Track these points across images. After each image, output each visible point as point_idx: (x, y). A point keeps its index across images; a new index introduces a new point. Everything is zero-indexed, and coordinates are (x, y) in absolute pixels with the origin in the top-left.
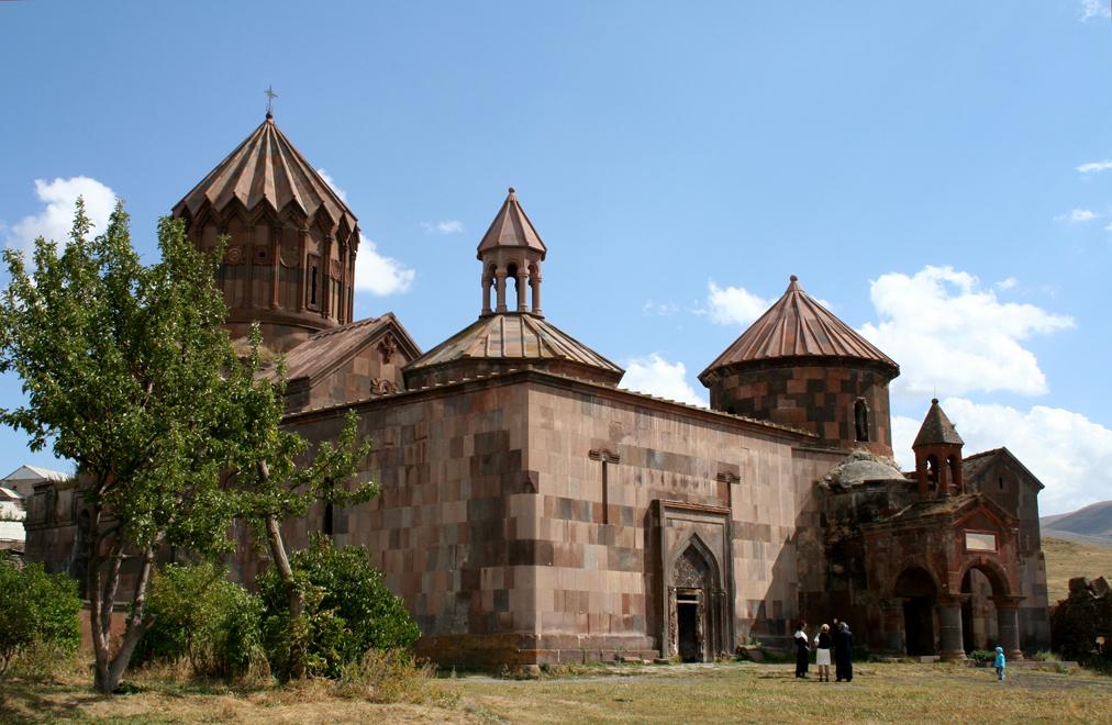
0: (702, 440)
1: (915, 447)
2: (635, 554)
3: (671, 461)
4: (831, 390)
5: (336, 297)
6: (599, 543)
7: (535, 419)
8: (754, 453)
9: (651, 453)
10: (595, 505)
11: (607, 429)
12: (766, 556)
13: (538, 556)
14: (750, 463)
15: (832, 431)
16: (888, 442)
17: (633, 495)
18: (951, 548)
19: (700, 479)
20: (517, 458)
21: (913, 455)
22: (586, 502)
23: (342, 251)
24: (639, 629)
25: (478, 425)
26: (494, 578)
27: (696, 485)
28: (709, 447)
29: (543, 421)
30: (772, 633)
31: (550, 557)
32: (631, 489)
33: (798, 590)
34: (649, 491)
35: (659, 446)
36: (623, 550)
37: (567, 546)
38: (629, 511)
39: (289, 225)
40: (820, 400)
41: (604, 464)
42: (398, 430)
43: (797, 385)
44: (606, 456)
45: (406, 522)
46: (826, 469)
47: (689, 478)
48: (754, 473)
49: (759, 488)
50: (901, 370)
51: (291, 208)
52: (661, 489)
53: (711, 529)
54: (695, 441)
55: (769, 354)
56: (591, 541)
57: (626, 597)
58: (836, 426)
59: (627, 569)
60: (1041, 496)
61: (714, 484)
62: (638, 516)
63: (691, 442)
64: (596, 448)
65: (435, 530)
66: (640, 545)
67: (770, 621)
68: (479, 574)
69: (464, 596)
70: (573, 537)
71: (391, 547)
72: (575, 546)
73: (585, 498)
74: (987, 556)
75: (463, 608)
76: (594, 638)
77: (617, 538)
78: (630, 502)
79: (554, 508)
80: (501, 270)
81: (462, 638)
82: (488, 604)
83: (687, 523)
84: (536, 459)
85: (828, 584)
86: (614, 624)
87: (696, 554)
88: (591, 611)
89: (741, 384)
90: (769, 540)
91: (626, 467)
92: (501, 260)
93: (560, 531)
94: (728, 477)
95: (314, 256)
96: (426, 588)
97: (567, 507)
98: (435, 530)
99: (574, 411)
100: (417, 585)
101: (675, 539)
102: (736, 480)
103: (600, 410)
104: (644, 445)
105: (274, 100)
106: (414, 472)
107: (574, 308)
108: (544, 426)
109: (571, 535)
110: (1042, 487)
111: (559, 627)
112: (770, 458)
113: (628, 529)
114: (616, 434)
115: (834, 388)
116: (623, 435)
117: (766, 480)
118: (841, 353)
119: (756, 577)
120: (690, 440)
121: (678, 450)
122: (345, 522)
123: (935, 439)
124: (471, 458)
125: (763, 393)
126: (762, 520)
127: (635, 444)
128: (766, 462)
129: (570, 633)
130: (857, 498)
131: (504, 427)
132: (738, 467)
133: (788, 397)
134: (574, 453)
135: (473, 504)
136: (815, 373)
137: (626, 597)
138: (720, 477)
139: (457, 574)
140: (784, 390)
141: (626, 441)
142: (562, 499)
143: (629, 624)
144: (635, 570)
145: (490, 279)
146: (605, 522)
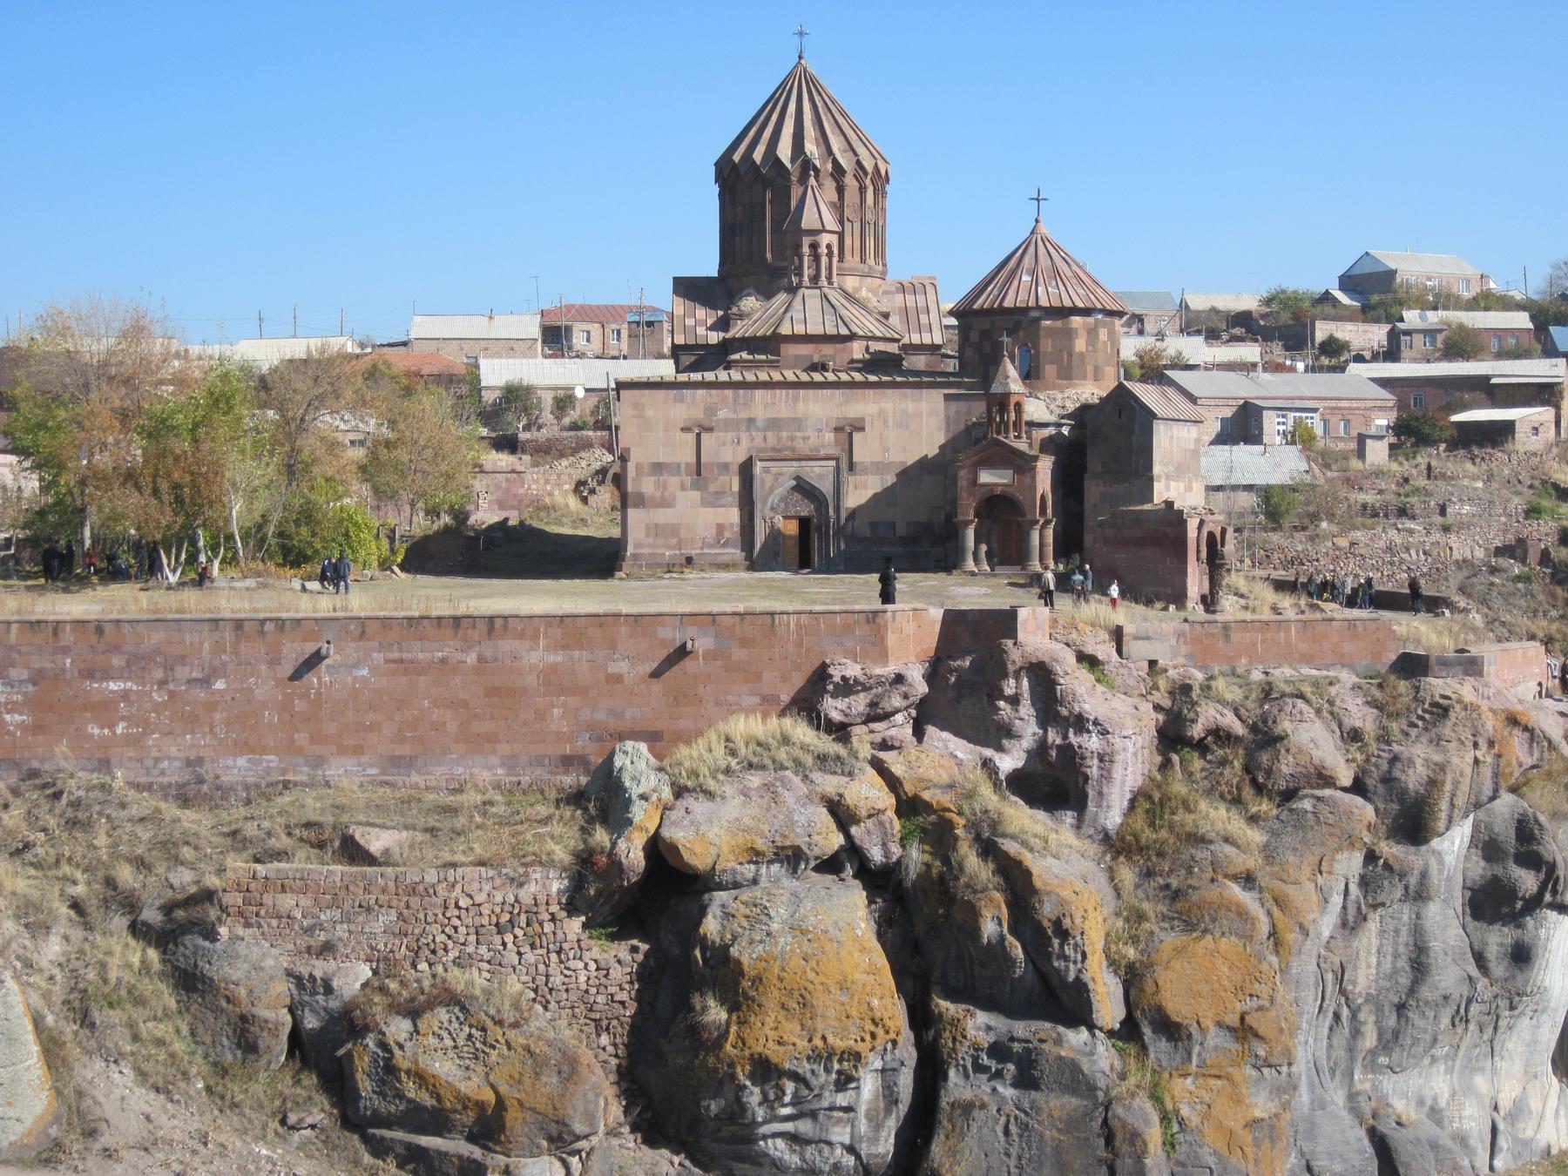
2: (732, 494)
3: (774, 424)
9: (751, 421)
31: (641, 501)
37: (658, 494)
38: (725, 467)
41: (698, 435)
44: (699, 430)
48: (886, 421)
56: (683, 488)
61: (830, 437)
62: (735, 468)
63: (801, 406)
64: (688, 424)
66: (736, 487)
70: (665, 487)
83: (791, 468)
94: (848, 430)
97: (658, 468)
101: (773, 484)
102: (862, 429)
104: (744, 415)
111: (650, 546)
112: (911, 407)
113: (723, 478)
114: (711, 411)
127: (732, 416)
132: (863, 420)
138: (838, 430)
146: (699, 473)
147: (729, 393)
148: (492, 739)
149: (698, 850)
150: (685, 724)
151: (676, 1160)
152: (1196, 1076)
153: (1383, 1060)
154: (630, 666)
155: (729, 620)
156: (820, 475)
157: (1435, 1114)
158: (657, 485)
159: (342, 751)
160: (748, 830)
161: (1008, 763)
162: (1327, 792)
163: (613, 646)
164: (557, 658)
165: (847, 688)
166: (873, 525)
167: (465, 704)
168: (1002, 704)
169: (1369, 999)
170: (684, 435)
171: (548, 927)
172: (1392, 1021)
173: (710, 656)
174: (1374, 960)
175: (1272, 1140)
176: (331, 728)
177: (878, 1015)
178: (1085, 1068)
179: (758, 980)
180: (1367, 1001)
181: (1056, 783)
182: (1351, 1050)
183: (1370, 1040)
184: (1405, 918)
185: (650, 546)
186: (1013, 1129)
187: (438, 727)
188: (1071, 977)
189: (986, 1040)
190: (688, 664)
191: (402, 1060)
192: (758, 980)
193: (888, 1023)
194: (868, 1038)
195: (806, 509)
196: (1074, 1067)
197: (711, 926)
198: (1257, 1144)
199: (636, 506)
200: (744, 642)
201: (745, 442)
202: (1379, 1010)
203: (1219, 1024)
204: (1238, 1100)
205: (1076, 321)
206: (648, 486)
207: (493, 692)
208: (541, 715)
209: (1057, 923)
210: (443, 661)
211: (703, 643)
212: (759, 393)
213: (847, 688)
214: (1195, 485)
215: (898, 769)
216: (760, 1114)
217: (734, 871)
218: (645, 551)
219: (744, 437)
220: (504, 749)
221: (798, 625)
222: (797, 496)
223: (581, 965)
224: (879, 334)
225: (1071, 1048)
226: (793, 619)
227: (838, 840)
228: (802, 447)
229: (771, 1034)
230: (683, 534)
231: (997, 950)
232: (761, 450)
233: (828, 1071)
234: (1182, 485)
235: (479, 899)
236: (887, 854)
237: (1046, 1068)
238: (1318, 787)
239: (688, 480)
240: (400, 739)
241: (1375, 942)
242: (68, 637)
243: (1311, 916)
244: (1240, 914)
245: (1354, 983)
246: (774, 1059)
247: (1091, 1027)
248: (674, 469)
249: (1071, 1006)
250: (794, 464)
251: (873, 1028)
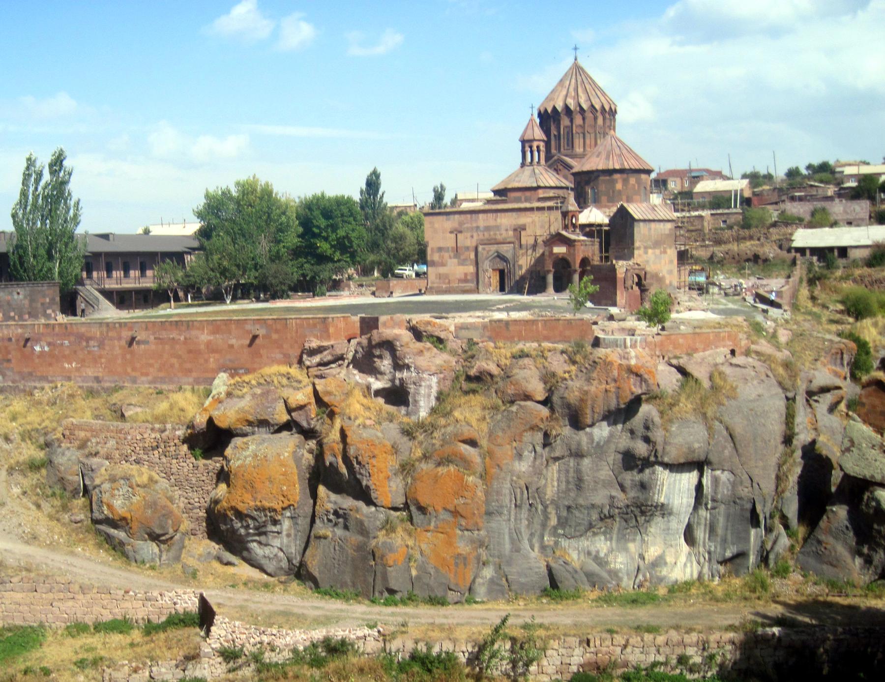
3: (488, 229)
9: (478, 228)
10: (452, 248)
19: (504, 232)
24: (472, 282)
36: (465, 260)
38: (467, 248)
44: (457, 232)
56: (450, 258)
61: (511, 233)
63: (499, 220)
66: (473, 256)
83: (494, 248)
86: (460, 281)
94: (519, 230)
97: (440, 249)
102: (524, 229)
104: (474, 225)
113: (467, 253)
114: (461, 224)
127: (469, 225)
138: (515, 230)
141: (466, 226)
143: (466, 281)
147: (469, 216)
148: (190, 371)
149: (222, 419)
150: (256, 366)
151: (217, 546)
152: (433, 531)
153: (560, 531)
154: (239, 341)
155: (270, 322)
156: (507, 250)
157: (597, 559)
158: (440, 257)
159: (142, 374)
160: (248, 412)
161: (377, 384)
162: (529, 403)
163: (230, 333)
164: (212, 338)
165: (312, 352)
167: (179, 357)
168: (376, 359)
169: (553, 502)
170: (449, 235)
171: (172, 449)
172: (565, 513)
173: (264, 337)
174: (556, 484)
175: (465, 564)
176: (138, 365)
177: (285, 493)
178: (366, 524)
179: (235, 475)
180: (552, 503)
181: (397, 395)
182: (544, 525)
183: (553, 521)
184: (572, 464)
186: (337, 548)
187: (172, 366)
188: (364, 483)
189: (330, 506)
190: (257, 341)
191: (106, 497)
192: (235, 475)
193: (290, 497)
194: (281, 503)
195: (501, 265)
196: (361, 523)
197: (228, 451)
198: (457, 565)
200: (277, 331)
201: (475, 237)
202: (557, 508)
203: (445, 509)
204: (450, 544)
205: (617, 176)
207: (190, 352)
208: (207, 361)
209: (357, 458)
210: (173, 339)
211: (261, 332)
212: (481, 216)
213: (312, 352)
214: (668, 251)
215: (318, 388)
216: (242, 531)
217: (241, 429)
218: (435, 285)
219: (475, 235)
220: (194, 374)
221: (296, 324)
222: (498, 260)
223: (184, 464)
224: (553, 185)
225: (363, 515)
226: (294, 321)
227: (285, 417)
229: (239, 498)
230: (451, 278)
231: (333, 468)
232: (482, 240)
233: (266, 516)
234: (657, 251)
235: (146, 436)
236: (309, 424)
237: (351, 524)
238: (525, 400)
239: (452, 254)
240: (160, 370)
241: (556, 475)
242: (57, 329)
243: (505, 462)
244: (461, 458)
245: (545, 494)
246: (240, 509)
247: (375, 505)
248: (446, 249)
249: (364, 495)
251: (283, 499)
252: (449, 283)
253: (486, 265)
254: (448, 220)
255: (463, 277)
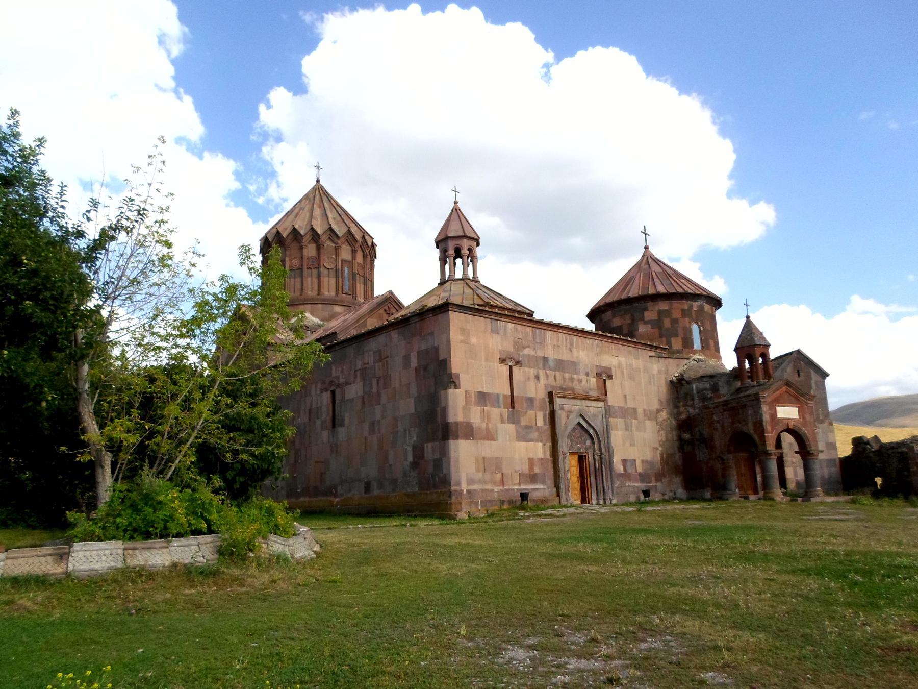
0: (583, 350)
1: (736, 350)
2: (538, 429)
3: (561, 365)
4: (674, 317)
5: (362, 286)
6: (509, 423)
7: (455, 336)
8: (622, 359)
9: (545, 359)
10: (505, 396)
11: (512, 343)
12: (634, 429)
13: (460, 434)
14: (620, 365)
15: (677, 344)
16: (717, 349)
17: (533, 390)
18: (766, 417)
19: (583, 377)
20: (444, 364)
21: (734, 355)
22: (498, 395)
23: (365, 256)
24: (543, 482)
25: (419, 345)
26: (433, 451)
27: (580, 381)
28: (591, 355)
29: (462, 338)
30: (642, 481)
31: (469, 432)
32: (532, 384)
33: (659, 452)
34: (546, 386)
35: (551, 354)
37: (484, 426)
38: (531, 401)
39: (329, 243)
40: (667, 323)
41: (510, 367)
42: (371, 353)
43: (650, 315)
45: (378, 416)
46: (675, 369)
47: (575, 376)
48: (623, 373)
49: (627, 383)
50: (723, 302)
51: (329, 232)
52: (554, 384)
53: (593, 409)
54: (578, 351)
55: (631, 294)
56: (503, 422)
57: (531, 461)
58: (680, 339)
59: (531, 441)
60: (828, 381)
61: (593, 380)
64: (504, 357)
65: (396, 419)
66: (540, 420)
67: (640, 474)
68: (423, 449)
69: (415, 465)
70: (489, 419)
71: (370, 434)
72: (490, 425)
73: (497, 391)
74: (793, 422)
75: (414, 474)
76: (507, 490)
77: (522, 419)
78: (531, 393)
79: (473, 398)
80: (451, 252)
81: (414, 494)
82: (430, 469)
83: (576, 406)
84: (457, 365)
85: (681, 448)
87: (584, 429)
88: (504, 471)
89: (614, 316)
90: (636, 419)
91: (527, 369)
92: (451, 246)
93: (478, 415)
94: (604, 376)
95: (346, 261)
96: (391, 461)
97: (483, 398)
98: (396, 419)
99: (485, 331)
100: (386, 458)
102: (610, 377)
103: (506, 326)
104: (540, 354)
105: (320, 171)
106: (382, 381)
107: (498, 272)
108: (462, 342)
109: (486, 417)
110: (827, 375)
113: (531, 413)
114: (519, 346)
115: (676, 314)
116: (524, 348)
117: (632, 378)
118: (680, 290)
119: (628, 444)
120: (574, 350)
121: (566, 356)
122: (343, 420)
123: (750, 345)
124: (416, 368)
125: (629, 322)
126: (631, 404)
127: (533, 353)
128: (631, 365)
129: (489, 487)
130: (697, 388)
131: (436, 345)
132: (610, 369)
133: (646, 323)
134: (487, 360)
135: (418, 400)
136: (663, 306)
137: (531, 461)
138: (599, 375)
139: (410, 449)
140: (642, 319)
141: (527, 351)
142: (479, 393)
144: (537, 441)
145: (443, 260)
146: (513, 407)
166: (624, 462)
185: (481, 482)
199: (467, 437)
206: (475, 416)
212: (549, 334)
219: (542, 373)
228: (579, 388)
239: (506, 412)
250: (578, 402)
252: (502, 482)
253: (564, 445)
254: (495, 331)
255: (525, 468)
